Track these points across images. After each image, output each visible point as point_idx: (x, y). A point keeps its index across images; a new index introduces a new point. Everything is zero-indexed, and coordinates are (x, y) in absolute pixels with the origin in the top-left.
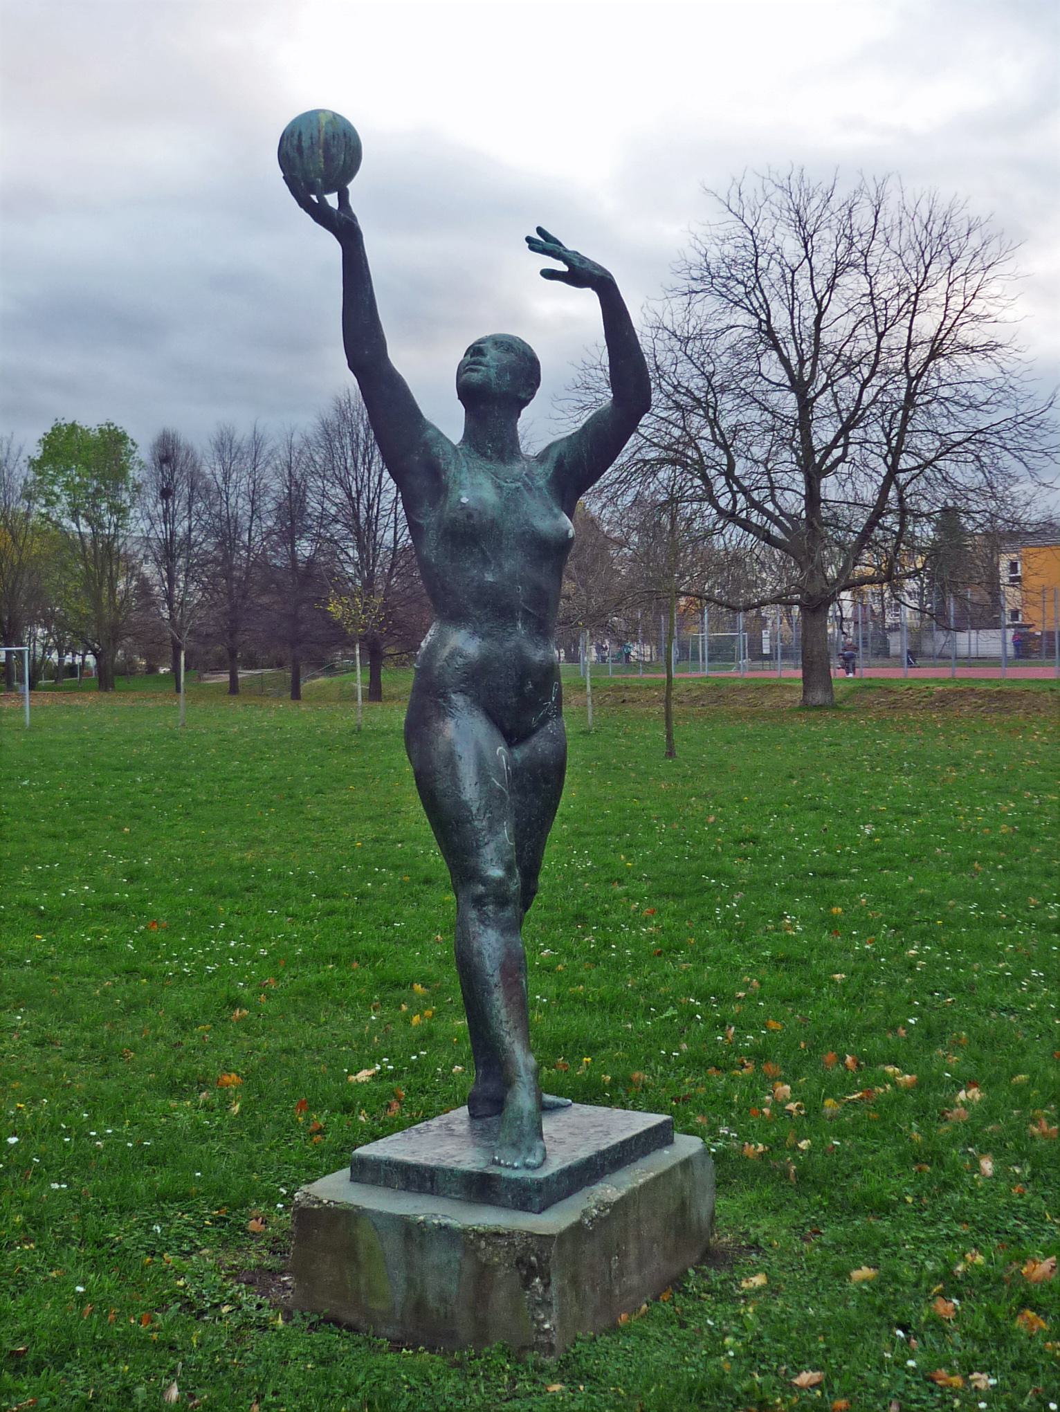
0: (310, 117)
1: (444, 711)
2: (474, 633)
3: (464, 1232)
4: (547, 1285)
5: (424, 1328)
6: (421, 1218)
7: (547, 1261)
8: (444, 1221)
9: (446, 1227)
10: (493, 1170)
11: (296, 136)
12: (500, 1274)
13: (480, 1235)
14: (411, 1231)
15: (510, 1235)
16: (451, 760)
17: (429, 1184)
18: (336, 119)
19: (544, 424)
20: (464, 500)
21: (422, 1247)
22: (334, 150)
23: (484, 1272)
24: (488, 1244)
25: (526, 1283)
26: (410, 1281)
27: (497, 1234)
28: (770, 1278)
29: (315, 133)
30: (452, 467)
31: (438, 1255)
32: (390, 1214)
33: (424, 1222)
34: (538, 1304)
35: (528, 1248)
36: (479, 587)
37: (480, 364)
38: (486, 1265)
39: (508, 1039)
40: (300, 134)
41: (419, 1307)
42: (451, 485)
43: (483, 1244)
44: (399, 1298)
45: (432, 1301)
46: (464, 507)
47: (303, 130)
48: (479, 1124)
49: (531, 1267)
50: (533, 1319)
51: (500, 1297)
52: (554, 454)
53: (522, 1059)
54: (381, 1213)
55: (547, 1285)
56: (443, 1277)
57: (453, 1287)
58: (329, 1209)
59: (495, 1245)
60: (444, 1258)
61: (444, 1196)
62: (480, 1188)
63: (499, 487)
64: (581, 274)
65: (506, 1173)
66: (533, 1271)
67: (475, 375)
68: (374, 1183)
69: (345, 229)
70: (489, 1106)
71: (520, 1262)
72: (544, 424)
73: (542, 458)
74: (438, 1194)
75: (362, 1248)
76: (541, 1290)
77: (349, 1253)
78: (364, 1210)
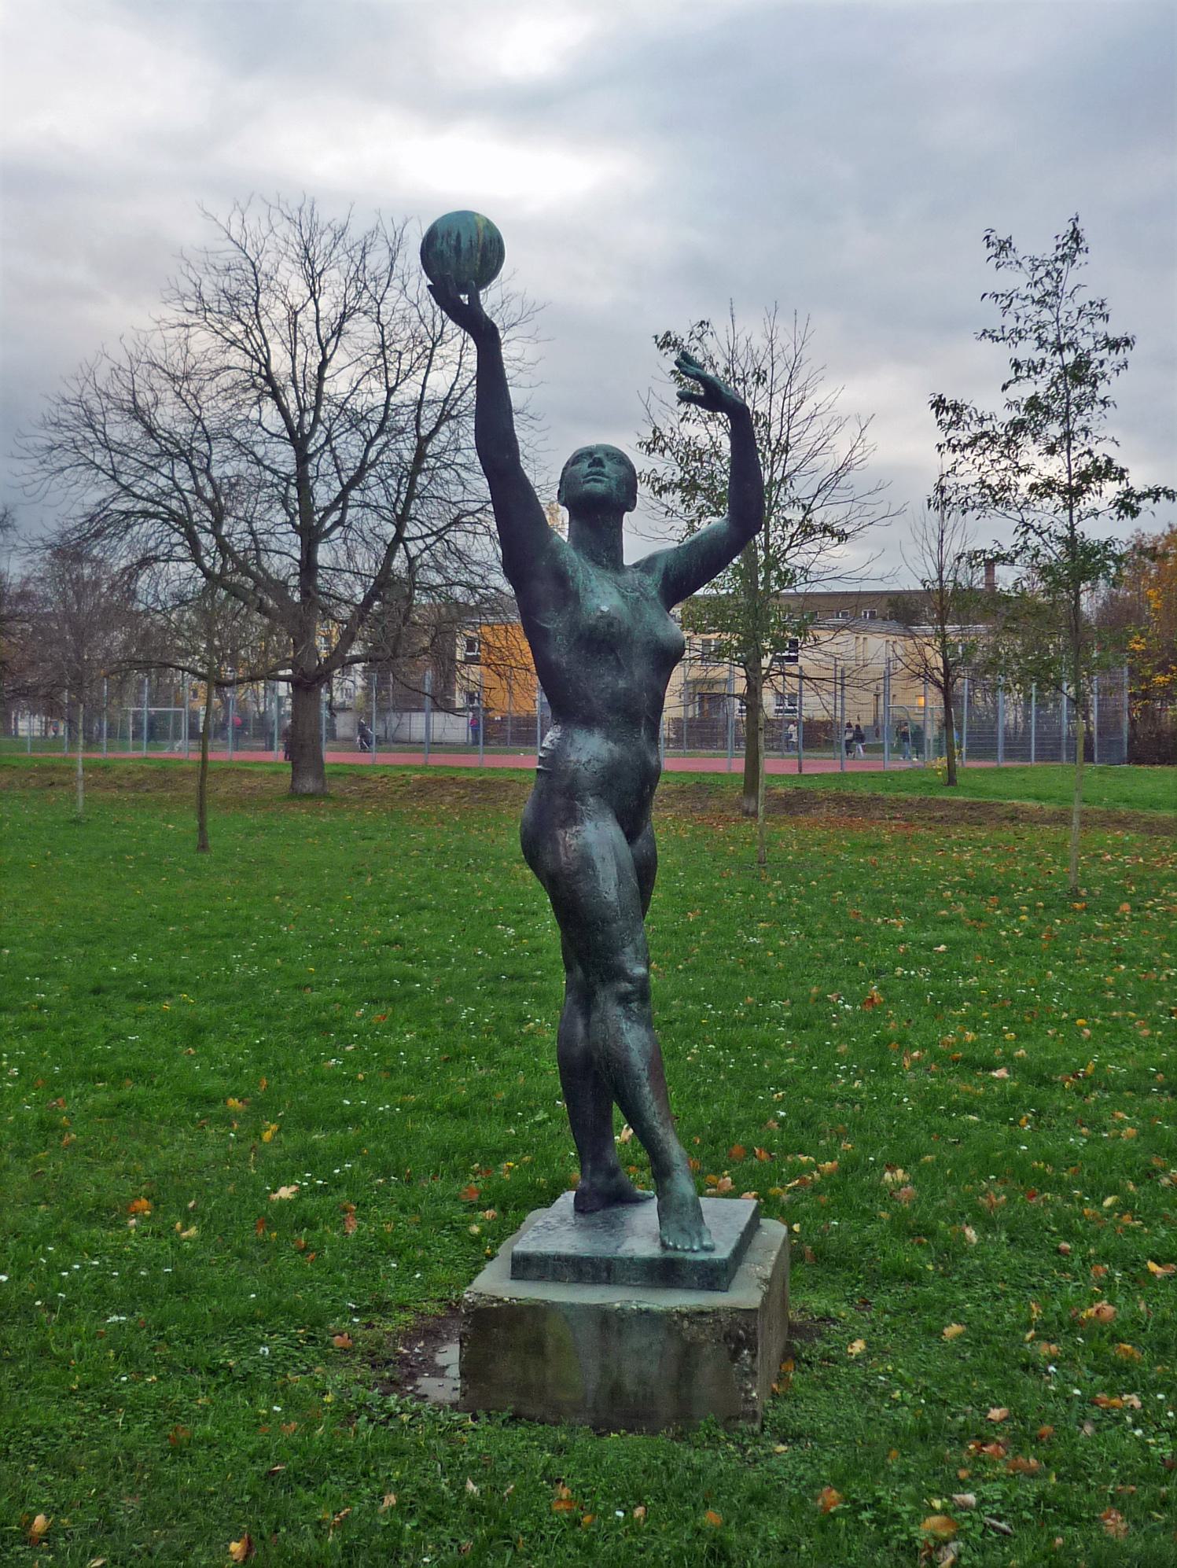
0: (465, 218)
1: (572, 818)
2: (608, 737)
3: (668, 1314)
4: (754, 1356)
5: (620, 1411)
6: (618, 1305)
7: (755, 1333)
8: (644, 1306)
9: (647, 1311)
10: (670, 1254)
11: (454, 236)
12: (707, 1350)
13: (683, 1316)
14: (607, 1320)
15: (715, 1312)
16: (586, 862)
17: (605, 1274)
18: (489, 226)
19: (650, 532)
20: (605, 608)
21: (620, 1333)
22: (490, 255)
23: (688, 1354)
24: (691, 1323)
25: (735, 1355)
26: (604, 1368)
27: (702, 1313)
28: (868, 1344)
29: (475, 238)
30: (580, 575)
31: (637, 1340)
32: (584, 1305)
33: (621, 1309)
34: (746, 1375)
35: (734, 1322)
36: (612, 694)
37: (602, 474)
38: (692, 1344)
39: (661, 1131)
40: (459, 236)
41: (616, 1392)
42: (581, 593)
43: (686, 1324)
44: (592, 1386)
45: (629, 1384)
46: (604, 615)
47: (462, 232)
48: (582, 1220)
49: (739, 1340)
50: (741, 1389)
51: (706, 1373)
52: (661, 565)
53: (675, 1151)
54: (573, 1305)
55: (754, 1356)
56: (642, 1364)
57: (654, 1369)
58: (512, 1306)
59: (700, 1324)
60: (645, 1341)
61: (622, 1284)
62: (665, 1272)
63: (623, 596)
64: (711, 396)
65: (689, 1256)
66: (741, 1343)
67: (599, 485)
68: (540, 1278)
69: (486, 336)
70: (605, 1199)
71: (727, 1336)
72: (650, 532)
73: (646, 566)
74: (615, 1283)
75: (550, 1342)
76: (749, 1361)
77: (536, 1347)
78: (553, 1303)
